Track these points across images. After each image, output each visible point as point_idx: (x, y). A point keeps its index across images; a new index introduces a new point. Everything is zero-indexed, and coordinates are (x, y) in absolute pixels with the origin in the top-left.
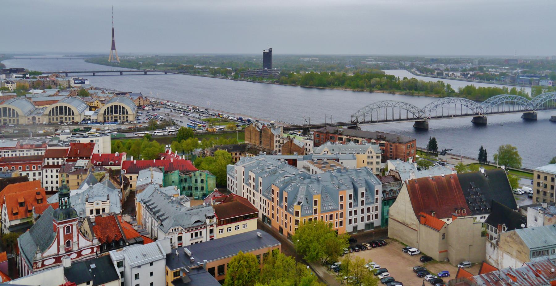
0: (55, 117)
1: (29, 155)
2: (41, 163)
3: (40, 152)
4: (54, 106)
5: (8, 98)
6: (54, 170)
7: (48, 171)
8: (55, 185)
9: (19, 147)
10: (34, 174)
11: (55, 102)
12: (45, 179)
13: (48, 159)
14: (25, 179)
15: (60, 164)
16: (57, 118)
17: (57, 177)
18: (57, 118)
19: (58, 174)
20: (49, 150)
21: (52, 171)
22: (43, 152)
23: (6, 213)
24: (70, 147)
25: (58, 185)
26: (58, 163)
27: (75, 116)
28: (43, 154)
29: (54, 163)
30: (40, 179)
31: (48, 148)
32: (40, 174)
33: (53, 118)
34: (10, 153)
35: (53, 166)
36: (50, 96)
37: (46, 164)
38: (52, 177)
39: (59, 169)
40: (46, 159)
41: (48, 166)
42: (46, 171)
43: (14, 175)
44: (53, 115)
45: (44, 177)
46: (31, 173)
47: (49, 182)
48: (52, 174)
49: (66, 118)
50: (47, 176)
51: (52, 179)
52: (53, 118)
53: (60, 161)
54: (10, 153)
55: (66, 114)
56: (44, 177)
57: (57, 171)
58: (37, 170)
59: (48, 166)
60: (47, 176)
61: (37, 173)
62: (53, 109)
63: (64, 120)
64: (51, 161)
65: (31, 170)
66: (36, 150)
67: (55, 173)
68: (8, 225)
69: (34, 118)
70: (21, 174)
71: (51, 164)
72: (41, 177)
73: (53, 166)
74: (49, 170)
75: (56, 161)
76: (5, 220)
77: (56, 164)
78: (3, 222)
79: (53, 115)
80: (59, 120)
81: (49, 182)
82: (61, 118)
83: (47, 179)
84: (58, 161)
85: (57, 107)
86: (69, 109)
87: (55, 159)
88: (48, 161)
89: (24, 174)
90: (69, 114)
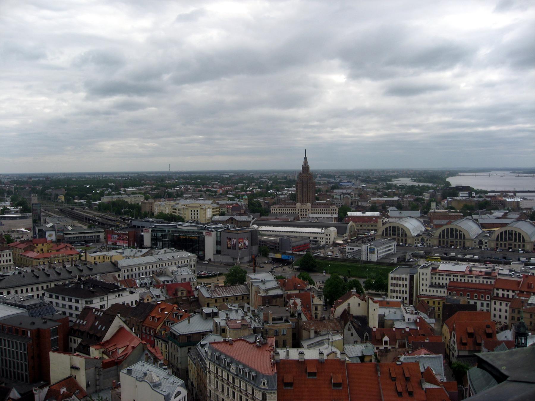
0: (503, 243)
1: (478, 282)
2: (489, 294)
3: (489, 281)
4: (503, 229)
5: (456, 218)
6: (504, 304)
7: (497, 303)
8: (503, 320)
9: (468, 273)
10: (482, 305)
11: (505, 225)
12: (493, 312)
13: (498, 289)
14: (474, 307)
15: (511, 297)
16: (505, 245)
17: (506, 311)
18: (505, 245)
19: (508, 308)
20: (499, 279)
21: (501, 304)
22: (493, 281)
23: (455, 340)
24: (522, 279)
25: (507, 321)
26: (508, 295)
27: (526, 244)
28: (493, 283)
29: (503, 295)
30: (488, 311)
31: (498, 277)
32: (488, 305)
33: (501, 244)
34: (459, 278)
35: (503, 299)
36: (498, 218)
37: (495, 295)
38: (500, 310)
39: (509, 304)
40: (495, 289)
41: (497, 298)
42: (495, 304)
43: (463, 300)
44: (501, 240)
45: (493, 309)
46: (479, 303)
47: (497, 316)
48: (501, 307)
49: (515, 245)
50: (495, 309)
51: (500, 313)
52: (501, 244)
53: (511, 294)
54: (459, 278)
55: (515, 241)
56: (493, 309)
57: (507, 305)
58: (485, 300)
59: (497, 298)
60: (495, 309)
61: (485, 303)
62: (501, 233)
63: (513, 246)
64: (500, 292)
65: (479, 299)
66: (485, 278)
67: (504, 307)
68: (456, 354)
69: (481, 242)
70: (469, 302)
71: (500, 295)
72: (489, 309)
73: (503, 299)
74: (498, 303)
75: (506, 293)
76: (454, 348)
77: (506, 296)
78: (452, 350)
79: (501, 240)
80: (507, 246)
81: (497, 316)
82: (509, 244)
83: (495, 312)
84: (508, 293)
85: (506, 232)
86: (520, 234)
87: (506, 291)
88: (498, 292)
89: (472, 302)
90: (519, 241)
